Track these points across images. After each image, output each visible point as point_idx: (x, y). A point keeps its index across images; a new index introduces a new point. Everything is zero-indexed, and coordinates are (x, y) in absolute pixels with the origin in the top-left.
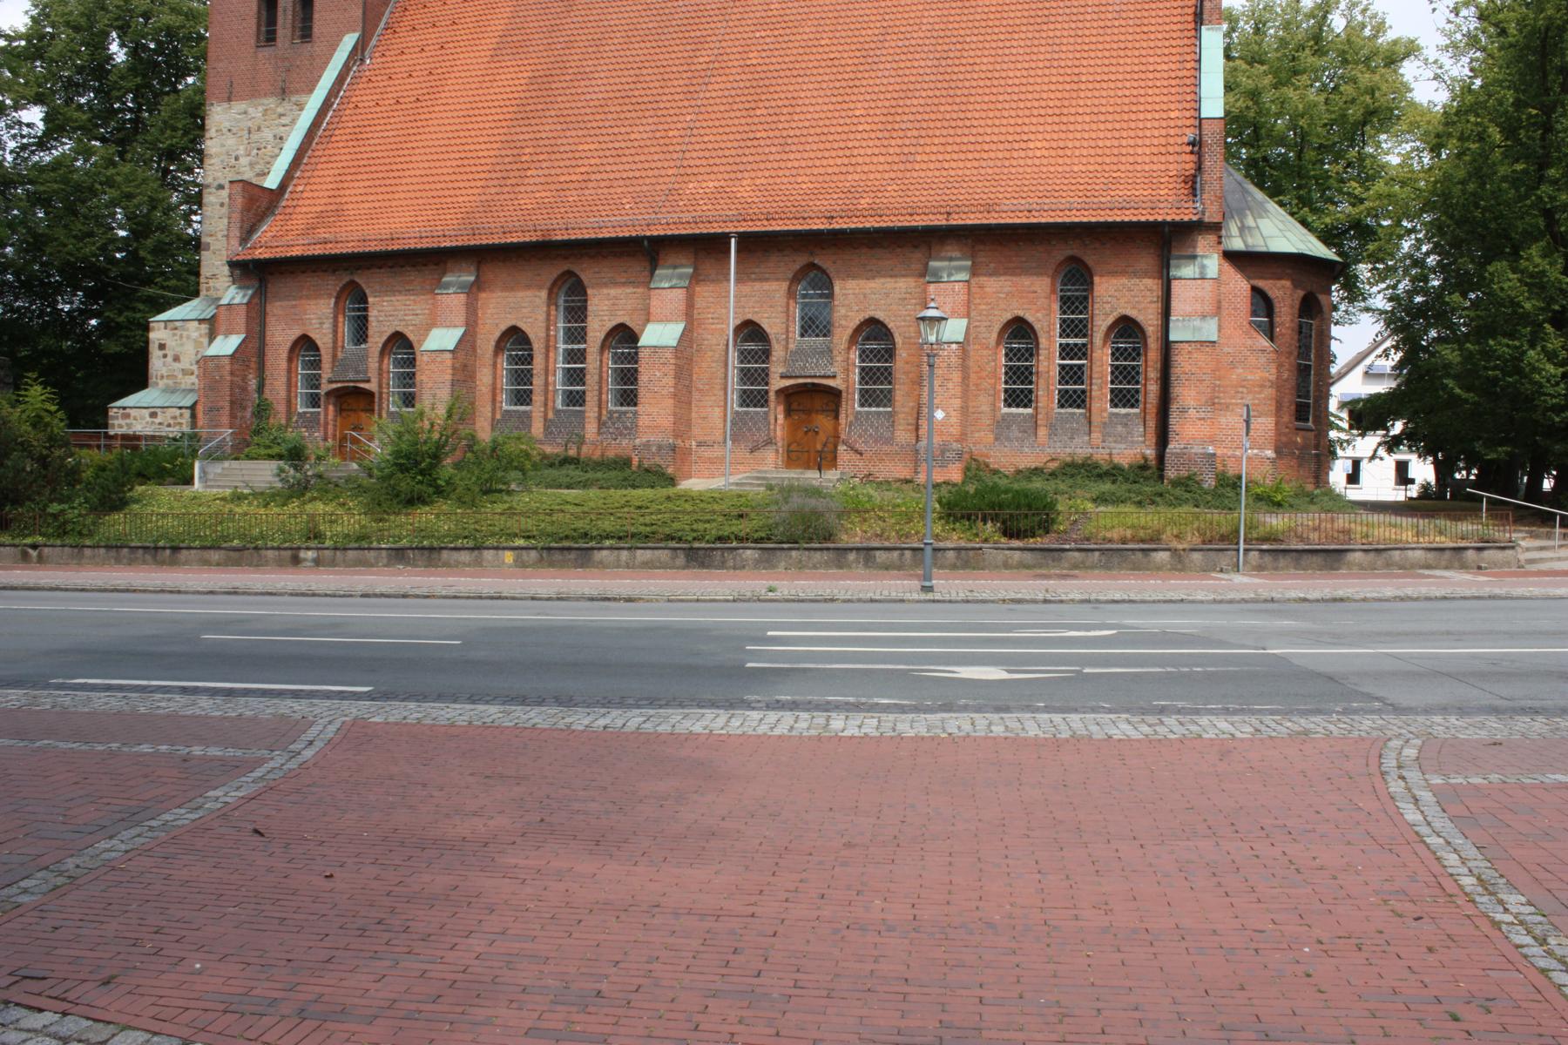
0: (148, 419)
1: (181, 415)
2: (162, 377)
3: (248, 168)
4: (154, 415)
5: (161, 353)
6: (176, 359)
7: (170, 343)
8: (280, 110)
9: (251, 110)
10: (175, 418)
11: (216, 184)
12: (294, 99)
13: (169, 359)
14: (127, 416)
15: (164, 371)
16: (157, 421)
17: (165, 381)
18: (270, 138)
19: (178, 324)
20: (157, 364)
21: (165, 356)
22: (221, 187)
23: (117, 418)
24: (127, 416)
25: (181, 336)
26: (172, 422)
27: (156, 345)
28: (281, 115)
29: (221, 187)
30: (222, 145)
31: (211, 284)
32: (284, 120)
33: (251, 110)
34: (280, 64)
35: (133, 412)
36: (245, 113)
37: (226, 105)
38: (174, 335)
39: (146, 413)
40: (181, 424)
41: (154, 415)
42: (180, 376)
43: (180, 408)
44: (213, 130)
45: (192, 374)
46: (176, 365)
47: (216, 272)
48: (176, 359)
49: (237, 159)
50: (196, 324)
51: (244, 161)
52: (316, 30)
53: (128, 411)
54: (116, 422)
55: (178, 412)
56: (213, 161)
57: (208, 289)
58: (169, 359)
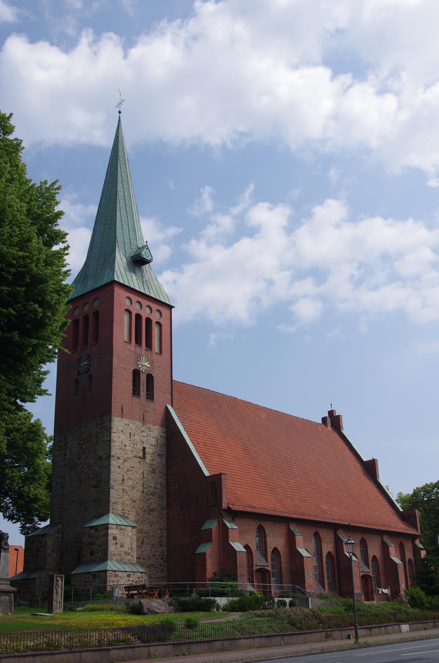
0: (127, 578)
1: (142, 576)
2: (115, 555)
3: (130, 452)
4: (129, 576)
5: (114, 542)
6: (122, 546)
7: (118, 537)
8: (142, 429)
9: (131, 425)
10: (139, 578)
11: (116, 456)
12: (148, 426)
13: (118, 545)
14: (117, 576)
15: (116, 552)
16: (131, 579)
17: (116, 557)
18: (139, 441)
19: (123, 527)
20: (112, 548)
21: (116, 544)
22: (119, 458)
23: (111, 577)
24: (117, 576)
25: (124, 534)
26: (138, 580)
27: (112, 537)
28: (143, 431)
29: (119, 458)
30: (119, 438)
31: (115, 507)
32: (144, 434)
33: (131, 425)
34: (142, 408)
35: (120, 574)
36: (129, 425)
37: (120, 419)
38: (121, 533)
39: (125, 574)
40: (142, 581)
41: (129, 576)
42: (123, 555)
43: (142, 573)
44: (115, 429)
45: (129, 554)
46: (122, 549)
47: (117, 501)
48: (122, 546)
49: (125, 446)
50: (130, 528)
51: (128, 448)
52: (155, 396)
53: (117, 573)
54: (111, 579)
55: (140, 575)
56: (115, 444)
57: (113, 509)
58: (118, 545)
